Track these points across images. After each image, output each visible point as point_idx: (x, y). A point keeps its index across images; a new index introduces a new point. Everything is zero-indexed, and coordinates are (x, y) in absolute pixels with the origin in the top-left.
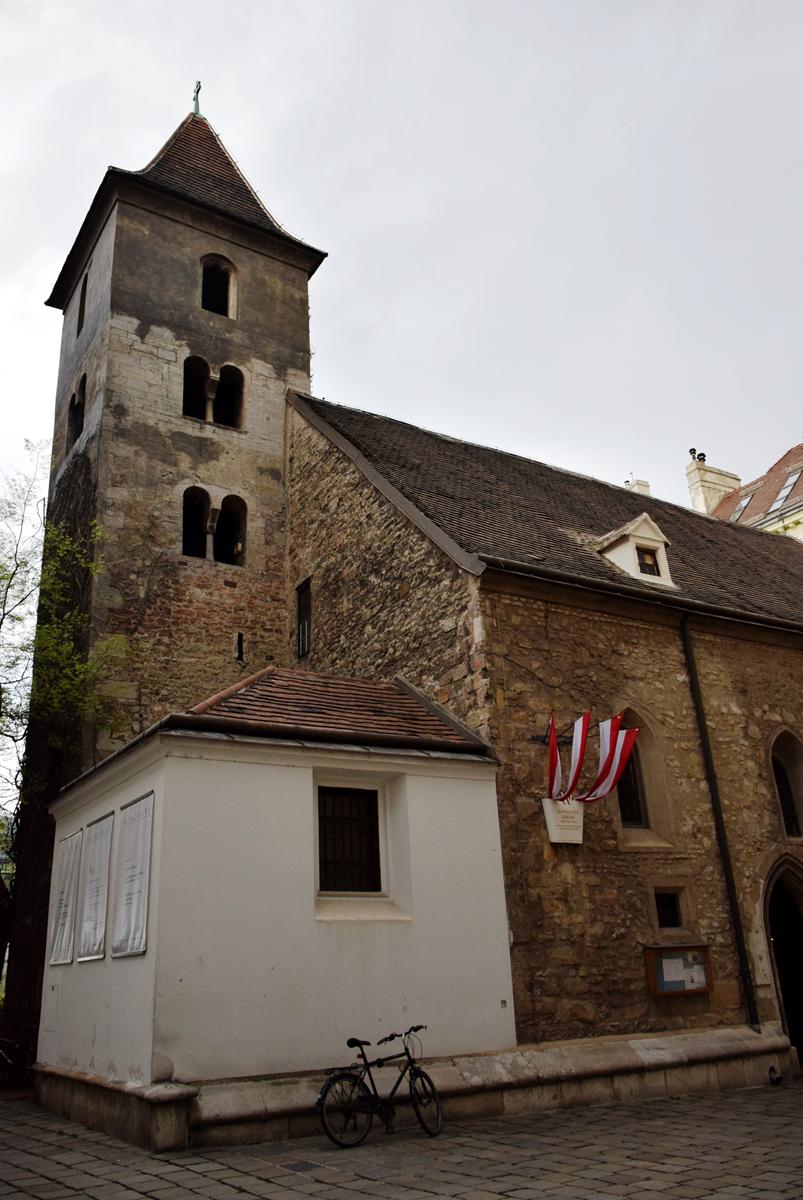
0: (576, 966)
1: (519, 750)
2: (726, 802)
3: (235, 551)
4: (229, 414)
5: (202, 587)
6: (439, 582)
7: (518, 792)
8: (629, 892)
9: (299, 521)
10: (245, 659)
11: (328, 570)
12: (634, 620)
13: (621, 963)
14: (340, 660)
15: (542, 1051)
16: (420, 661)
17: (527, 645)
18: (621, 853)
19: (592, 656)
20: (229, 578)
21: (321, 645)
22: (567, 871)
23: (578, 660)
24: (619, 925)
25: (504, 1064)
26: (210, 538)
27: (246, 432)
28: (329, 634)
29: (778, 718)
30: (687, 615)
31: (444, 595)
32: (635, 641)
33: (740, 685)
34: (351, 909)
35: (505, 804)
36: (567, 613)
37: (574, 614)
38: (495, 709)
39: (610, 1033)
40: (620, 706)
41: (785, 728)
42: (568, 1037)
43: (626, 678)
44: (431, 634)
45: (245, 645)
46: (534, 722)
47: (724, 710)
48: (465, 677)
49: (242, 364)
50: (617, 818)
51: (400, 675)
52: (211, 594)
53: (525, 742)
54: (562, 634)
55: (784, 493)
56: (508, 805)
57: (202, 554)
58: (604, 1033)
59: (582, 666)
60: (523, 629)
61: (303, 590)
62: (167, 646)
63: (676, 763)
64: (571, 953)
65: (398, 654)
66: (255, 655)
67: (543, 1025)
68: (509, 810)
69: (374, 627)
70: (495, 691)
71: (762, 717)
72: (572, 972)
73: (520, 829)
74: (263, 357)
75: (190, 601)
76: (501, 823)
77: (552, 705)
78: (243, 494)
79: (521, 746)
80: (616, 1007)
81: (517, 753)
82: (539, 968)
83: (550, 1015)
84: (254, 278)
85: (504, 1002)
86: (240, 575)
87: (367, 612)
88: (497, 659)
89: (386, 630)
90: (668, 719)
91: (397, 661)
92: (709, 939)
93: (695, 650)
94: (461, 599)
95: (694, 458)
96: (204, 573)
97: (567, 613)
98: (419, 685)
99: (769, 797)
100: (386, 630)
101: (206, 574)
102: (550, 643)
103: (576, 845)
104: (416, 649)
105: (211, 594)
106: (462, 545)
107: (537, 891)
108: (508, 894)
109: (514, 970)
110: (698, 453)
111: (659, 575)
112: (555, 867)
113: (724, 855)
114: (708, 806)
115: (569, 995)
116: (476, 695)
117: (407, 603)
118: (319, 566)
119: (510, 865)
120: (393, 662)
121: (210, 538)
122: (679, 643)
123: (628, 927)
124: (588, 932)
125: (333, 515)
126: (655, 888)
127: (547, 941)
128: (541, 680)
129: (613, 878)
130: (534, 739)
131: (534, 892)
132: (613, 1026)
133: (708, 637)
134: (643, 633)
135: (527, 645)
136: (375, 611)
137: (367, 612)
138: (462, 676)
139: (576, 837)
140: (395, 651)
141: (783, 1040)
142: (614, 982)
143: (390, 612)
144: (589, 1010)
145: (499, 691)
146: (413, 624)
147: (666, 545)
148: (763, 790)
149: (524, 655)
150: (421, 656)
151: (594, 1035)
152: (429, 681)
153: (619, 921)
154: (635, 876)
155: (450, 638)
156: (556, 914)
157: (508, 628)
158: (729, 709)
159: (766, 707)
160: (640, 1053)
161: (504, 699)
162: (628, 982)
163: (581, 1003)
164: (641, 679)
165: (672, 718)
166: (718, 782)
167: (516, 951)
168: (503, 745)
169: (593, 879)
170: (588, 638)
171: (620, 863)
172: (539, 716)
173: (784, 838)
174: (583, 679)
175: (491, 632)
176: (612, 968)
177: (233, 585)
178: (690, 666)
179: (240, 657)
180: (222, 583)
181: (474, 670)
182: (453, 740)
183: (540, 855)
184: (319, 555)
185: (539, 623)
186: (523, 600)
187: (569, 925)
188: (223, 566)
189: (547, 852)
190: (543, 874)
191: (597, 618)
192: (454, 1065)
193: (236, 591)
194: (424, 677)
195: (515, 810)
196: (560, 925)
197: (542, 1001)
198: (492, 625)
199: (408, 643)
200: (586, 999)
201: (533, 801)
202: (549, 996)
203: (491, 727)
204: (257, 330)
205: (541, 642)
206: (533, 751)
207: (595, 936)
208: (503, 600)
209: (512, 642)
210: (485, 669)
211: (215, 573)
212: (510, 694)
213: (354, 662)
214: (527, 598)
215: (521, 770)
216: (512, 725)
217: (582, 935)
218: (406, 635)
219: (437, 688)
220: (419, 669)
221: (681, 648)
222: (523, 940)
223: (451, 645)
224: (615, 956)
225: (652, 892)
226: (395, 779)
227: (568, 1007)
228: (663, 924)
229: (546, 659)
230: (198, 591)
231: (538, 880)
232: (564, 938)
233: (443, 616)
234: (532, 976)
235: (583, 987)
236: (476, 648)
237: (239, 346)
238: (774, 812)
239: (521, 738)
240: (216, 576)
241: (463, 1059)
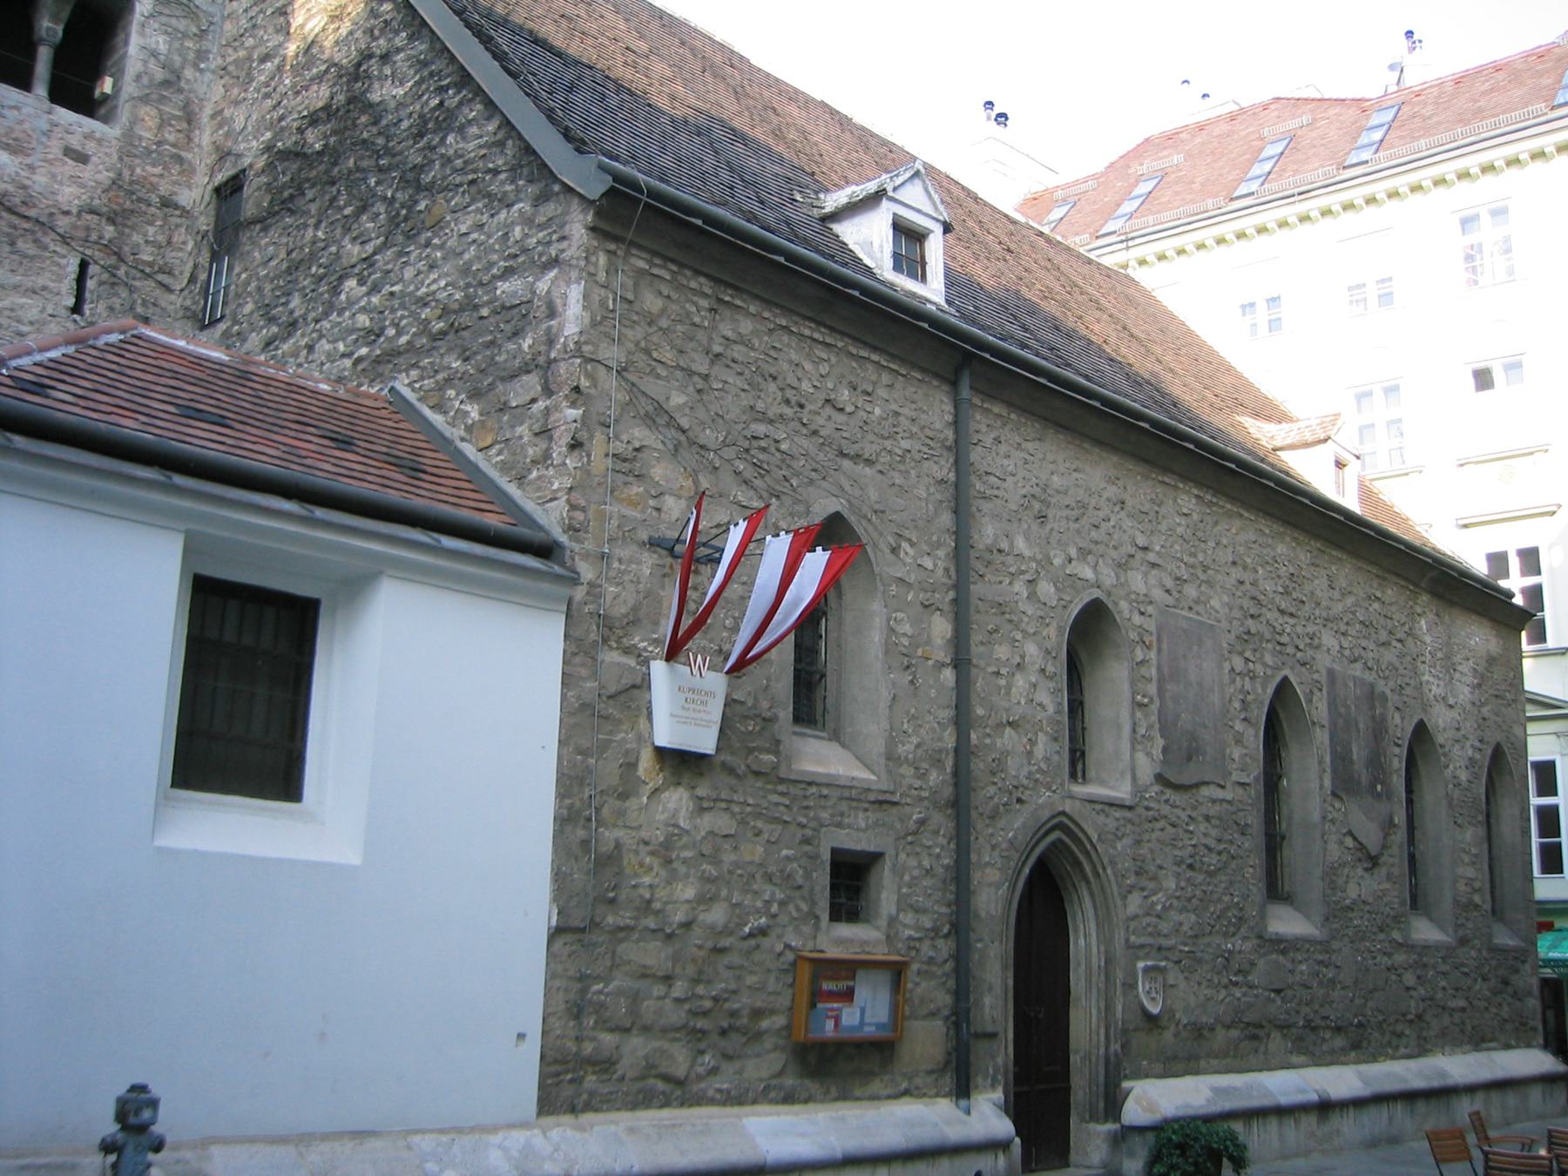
0: (668, 979)
1: (620, 561)
2: (980, 711)
3: (97, 93)
6: (509, 206)
7: (605, 640)
8: (785, 852)
9: (242, 53)
10: (87, 312)
12: (875, 349)
13: (751, 980)
14: (284, 340)
15: (582, 1129)
16: (446, 359)
17: (668, 355)
18: (782, 781)
19: (788, 402)
20: (75, 142)
22: (677, 800)
23: (760, 406)
24: (758, 911)
25: (505, 1150)
26: (44, 56)
28: (268, 287)
29: (1088, 574)
30: (968, 356)
31: (517, 232)
32: (870, 389)
33: (1037, 506)
34: (230, 826)
35: (577, 660)
36: (752, 309)
37: (766, 314)
38: (586, 471)
39: (712, 1102)
40: (823, 506)
41: (1096, 593)
42: (633, 1106)
43: (842, 454)
44: (476, 307)
45: (90, 284)
46: (658, 510)
47: (1004, 545)
48: (534, 401)
50: (786, 713)
51: (402, 384)
53: (634, 548)
54: (736, 347)
55: (1128, 207)
56: (583, 665)
58: (700, 1100)
59: (763, 418)
60: (664, 323)
61: (229, 191)
63: (907, 628)
64: (663, 955)
65: (403, 340)
66: (111, 309)
67: (591, 1081)
68: (584, 672)
69: (362, 282)
70: (591, 437)
71: (1063, 567)
72: (658, 990)
73: (598, 710)
76: (563, 696)
77: (696, 483)
79: (624, 553)
80: (727, 1057)
81: (616, 565)
82: (598, 978)
83: (605, 1065)
85: (521, 1036)
86: (100, 141)
87: (354, 251)
88: (602, 371)
89: (387, 289)
90: (905, 545)
91: (400, 353)
92: (910, 948)
93: (973, 426)
94: (549, 243)
95: (989, 118)
96: (21, 122)
97: (752, 309)
98: (438, 407)
99: (1051, 709)
100: (387, 289)
101: (26, 126)
102: (712, 362)
103: (703, 756)
104: (443, 333)
105: (31, 168)
106: (567, 135)
107: (619, 833)
108: (558, 834)
109: (551, 976)
110: (997, 110)
111: (924, 279)
112: (656, 791)
113: (959, 803)
114: (947, 714)
115: (646, 1029)
116: (551, 438)
117: (436, 241)
119: (570, 781)
120: (392, 354)
121: (44, 56)
122: (949, 408)
123: (774, 916)
124: (701, 917)
126: (834, 851)
127: (621, 929)
128: (684, 432)
129: (759, 824)
130: (654, 544)
131: (610, 835)
132: (720, 1091)
133: (997, 409)
134: (886, 378)
135: (668, 355)
136: (369, 248)
138: (528, 398)
139: (704, 741)
140: (399, 334)
141: (1003, 1127)
142: (733, 1014)
143: (401, 254)
144: (681, 1059)
145: (599, 437)
146: (440, 285)
147: (947, 228)
148: (1042, 696)
149: (658, 377)
150: (450, 350)
151: (682, 1105)
153: (759, 904)
154: (804, 826)
155: (518, 316)
156: (647, 880)
157: (635, 318)
158: (1012, 546)
159: (1073, 552)
160: (760, 1140)
161: (607, 455)
162: (757, 1014)
163: (666, 1045)
164: (869, 462)
165: (912, 545)
166: (974, 671)
167: (558, 944)
168: (589, 545)
169: (722, 822)
170: (785, 366)
171: (775, 798)
172: (669, 501)
173: (1062, 785)
174: (763, 444)
175: (599, 321)
176: (733, 986)
177: (82, 158)
178: (959, 450)
179: (77, 309)
180: (55, 150)
181: (553, 387)
182: (493, 521)
183: (633, 765)
185: (697, 320)
186: (674, 268)
187: (666, 903)
188: (64, 115)
189: (646, 760)
190: (633, 803)
191: (807, 332)
192: (409, 1148)
193: (87, 173)
194: (451, 393)
195: (594, 675)
196: (649, 902)
197: (594, 1039)
198: (603, 303)
199: (427, 321)
200: (675, 1040)
201: (632, 662)
202: (612, 1030)
203: (573, 507)
205: (695, 356)
206: (648, 562)
207: (712, 927)
208: (635, 261)
209: (637, 344)
210: (577, 389)
211: (46, 127)
212: (619, 447)
213: (310, 348)
214: (682, 265)
215: (618, 599)
216: (613, 509)
217: (687, 925)
218: (426, 305)
220: (440, 377)
221: (949, 418)
222: (576, 922)
223: (517, 334)
224: (741, 967)
225: (826, 856)
226: (356, 586)
227: (641, 1053)
228: (835, 916)
229: (699, 391)
231: (621, 813)
232: (652, 925)
233: (508, 273)
234: (584, 991)
235: (676, 1016)
236: (565, 345)
238: (1056, 740)
239: (625, 534)
240: (47, 134)
241: (427, 1137)
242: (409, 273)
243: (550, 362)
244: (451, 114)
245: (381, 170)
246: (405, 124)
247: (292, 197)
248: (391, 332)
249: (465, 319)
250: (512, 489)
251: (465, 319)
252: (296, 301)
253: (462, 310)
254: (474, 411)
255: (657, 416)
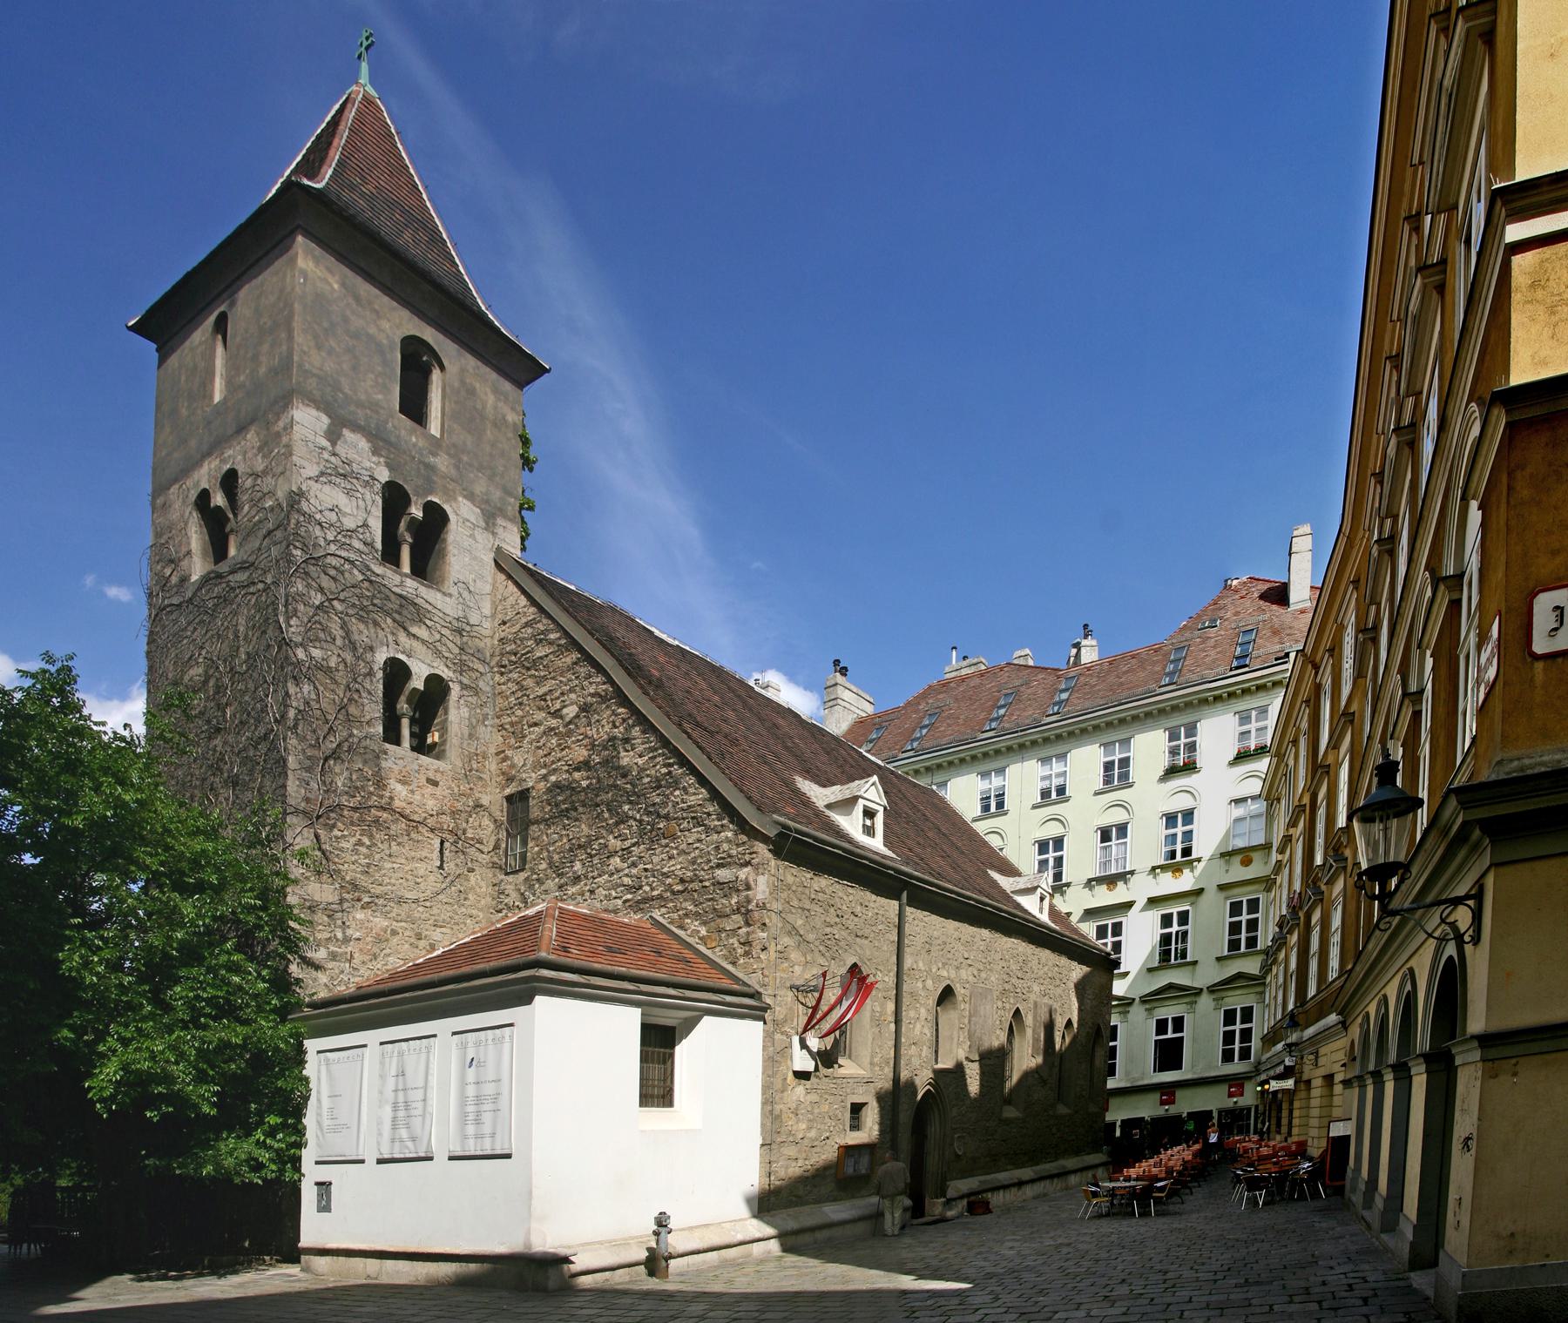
4: (426, 564)
5: (403, 782)
11: (557, 785)
17: (795, 903)
20: (431, 775)
21: (544, 866)
26: (405, 722)
27: (450, 595)
28: (556, 857)
31: (725, 846)
49: (447, 501)
51: (657, 914)
52: (412, 792)
57: (398, 742)
61: (518, 800)
62: (368, 847)
69: (623, 860)
74: (471, 497)
75: (391, 798)
78: (446, 673)
84: (463, 382)
87: (614, 843)
98: (681, 927)
105: (412, 792)
118: (545, 777)
121: (405, 722)
125: (570, 722)
136: (627, 844)
137: (614, 843)
146: (677, 866)
152: (694, 925)
177: (435, 784)
184: (545, 766)
188: (424, 760)
204: (465, 458)
213: (592, 892)
219: (703, 932)
230: (399, 787)
233: (719, 866)
237: (444, 477)
240: (418, 771)
242: (656, 859)
243: (748, 911)
244: (677, 782)
245: (631, 802)
246: (646, 780)
247: (567, 810)
248: (647, 888)
249: (696, 886)
250: (730, 967)
251: (696, 886)
252: (578, 866)
253: (692, 881)
254: (703, 932)
255: (793, 931)
